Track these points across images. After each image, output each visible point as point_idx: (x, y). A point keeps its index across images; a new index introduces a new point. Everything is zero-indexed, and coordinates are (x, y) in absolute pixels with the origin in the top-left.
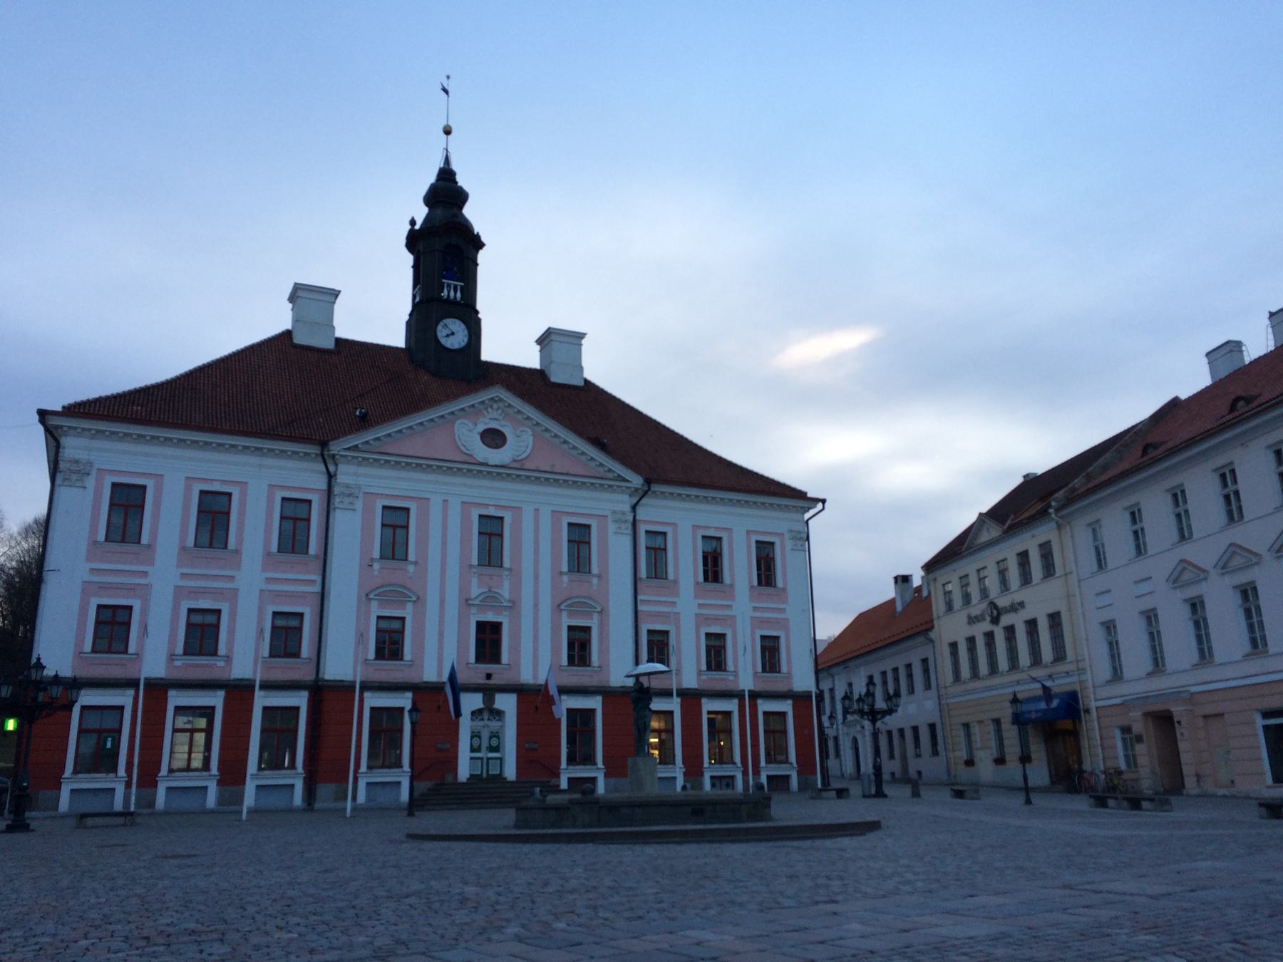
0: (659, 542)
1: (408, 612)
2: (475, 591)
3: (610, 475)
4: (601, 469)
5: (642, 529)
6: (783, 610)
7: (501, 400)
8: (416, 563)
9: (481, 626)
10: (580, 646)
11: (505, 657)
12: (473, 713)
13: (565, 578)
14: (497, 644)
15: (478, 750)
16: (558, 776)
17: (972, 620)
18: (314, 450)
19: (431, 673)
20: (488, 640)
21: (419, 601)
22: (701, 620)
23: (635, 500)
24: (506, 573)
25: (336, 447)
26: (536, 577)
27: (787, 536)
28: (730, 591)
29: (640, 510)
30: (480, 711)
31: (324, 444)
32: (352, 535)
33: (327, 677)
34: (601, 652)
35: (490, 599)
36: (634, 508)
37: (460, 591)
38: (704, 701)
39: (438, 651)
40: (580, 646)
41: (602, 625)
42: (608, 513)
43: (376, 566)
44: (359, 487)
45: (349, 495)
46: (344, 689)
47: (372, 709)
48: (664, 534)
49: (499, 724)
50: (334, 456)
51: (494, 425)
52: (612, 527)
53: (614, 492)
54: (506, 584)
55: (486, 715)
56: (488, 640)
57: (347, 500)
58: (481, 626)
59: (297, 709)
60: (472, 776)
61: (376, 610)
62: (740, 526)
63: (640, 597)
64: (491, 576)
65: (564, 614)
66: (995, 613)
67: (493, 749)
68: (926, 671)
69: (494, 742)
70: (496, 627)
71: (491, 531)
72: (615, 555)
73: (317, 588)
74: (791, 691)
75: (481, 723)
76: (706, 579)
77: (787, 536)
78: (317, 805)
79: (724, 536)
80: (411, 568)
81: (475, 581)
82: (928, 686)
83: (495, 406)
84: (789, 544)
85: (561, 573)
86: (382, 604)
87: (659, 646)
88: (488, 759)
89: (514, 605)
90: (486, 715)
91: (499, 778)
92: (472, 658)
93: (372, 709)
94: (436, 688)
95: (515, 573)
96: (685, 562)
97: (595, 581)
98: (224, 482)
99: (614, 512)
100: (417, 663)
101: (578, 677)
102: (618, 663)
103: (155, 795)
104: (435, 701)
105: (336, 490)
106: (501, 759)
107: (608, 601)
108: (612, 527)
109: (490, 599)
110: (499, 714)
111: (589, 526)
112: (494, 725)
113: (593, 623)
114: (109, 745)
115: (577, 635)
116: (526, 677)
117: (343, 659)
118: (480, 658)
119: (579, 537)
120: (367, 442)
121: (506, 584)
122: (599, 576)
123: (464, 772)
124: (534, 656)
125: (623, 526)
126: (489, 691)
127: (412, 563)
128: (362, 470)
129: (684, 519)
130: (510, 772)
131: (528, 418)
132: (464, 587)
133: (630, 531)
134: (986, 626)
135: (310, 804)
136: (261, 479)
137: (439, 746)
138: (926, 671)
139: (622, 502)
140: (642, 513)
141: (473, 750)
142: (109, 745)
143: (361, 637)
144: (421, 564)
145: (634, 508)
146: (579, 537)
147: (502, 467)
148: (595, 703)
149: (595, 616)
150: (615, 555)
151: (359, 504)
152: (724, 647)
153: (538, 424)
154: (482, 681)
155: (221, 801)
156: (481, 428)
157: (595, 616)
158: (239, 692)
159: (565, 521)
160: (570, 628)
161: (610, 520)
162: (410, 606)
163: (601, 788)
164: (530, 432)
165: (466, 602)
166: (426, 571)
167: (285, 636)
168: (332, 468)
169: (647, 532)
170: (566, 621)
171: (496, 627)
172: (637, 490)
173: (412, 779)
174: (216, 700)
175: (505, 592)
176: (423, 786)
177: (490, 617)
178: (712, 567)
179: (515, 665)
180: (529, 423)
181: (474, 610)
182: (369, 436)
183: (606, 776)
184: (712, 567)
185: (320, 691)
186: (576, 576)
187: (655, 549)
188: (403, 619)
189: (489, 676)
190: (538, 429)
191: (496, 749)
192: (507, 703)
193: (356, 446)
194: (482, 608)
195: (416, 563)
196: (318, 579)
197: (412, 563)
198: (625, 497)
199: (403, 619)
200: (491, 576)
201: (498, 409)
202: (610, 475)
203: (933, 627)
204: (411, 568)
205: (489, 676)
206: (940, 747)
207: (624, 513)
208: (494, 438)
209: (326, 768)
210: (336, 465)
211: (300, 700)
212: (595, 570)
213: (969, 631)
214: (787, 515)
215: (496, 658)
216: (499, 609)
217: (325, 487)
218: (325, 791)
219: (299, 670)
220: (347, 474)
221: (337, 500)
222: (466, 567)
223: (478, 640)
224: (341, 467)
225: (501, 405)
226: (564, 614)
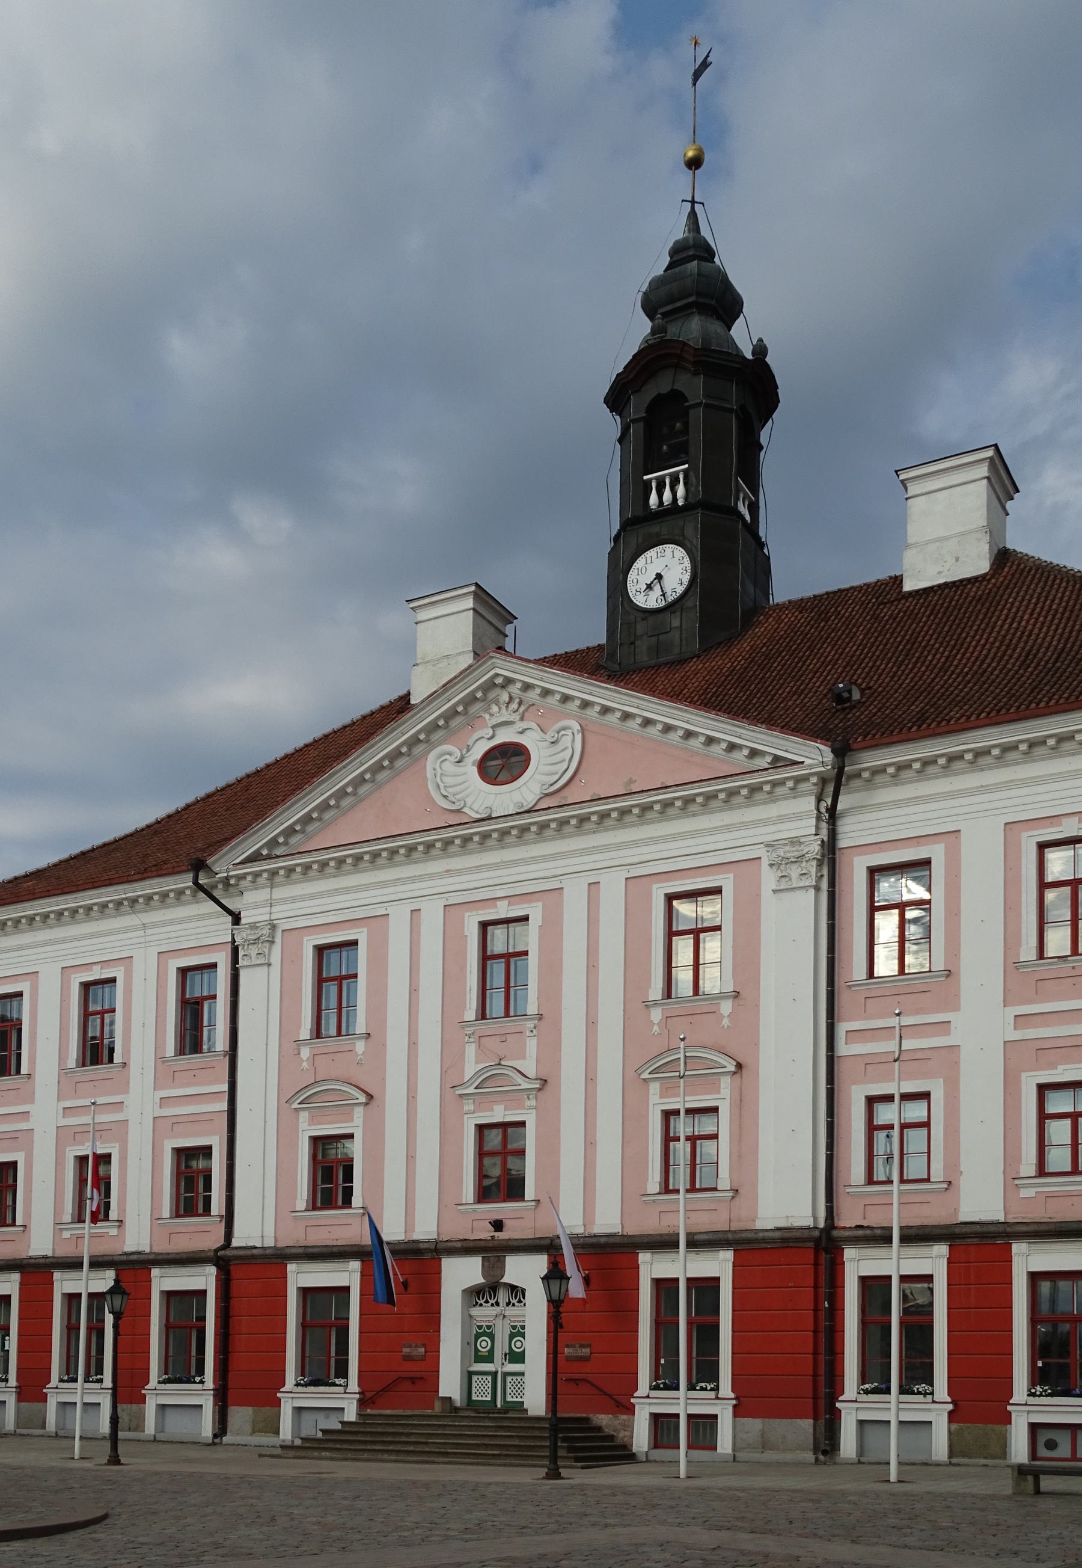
1: (356, 1123)
2: (471, 1067)
7: (509, 681)
19: (393, 1231)
26: (591, 1023)
35: (490, 1082)
37: (444, 1073)
41: (745, 1106)
42: (760, 852)
46: (274, 1261)
51: (505, 736)
59: (203, 1293)
61: (308, 1128)
64: (503, 1037)
65: (654, 1088)
81: (471, 1050)
85: (648, 1005)
95: (547, 1021)
118: (484, 1194)
131: (566, 699)
132: (450, 1062)
140: (850, 833)
143: (284, 1172)
149: (725, 1082)
162: (359, 1111)
167: (193, 1180)
177: (499, 1114)
179: (549, 1200)
181: (469, 1106)
200: (503, 1037)
208: (505, 762)
209: (246, 1384)
211: (204, 1279)
216: (514, 1096)
218: (240, 1416)
219: (204, 1234)
226: (654, 1088)
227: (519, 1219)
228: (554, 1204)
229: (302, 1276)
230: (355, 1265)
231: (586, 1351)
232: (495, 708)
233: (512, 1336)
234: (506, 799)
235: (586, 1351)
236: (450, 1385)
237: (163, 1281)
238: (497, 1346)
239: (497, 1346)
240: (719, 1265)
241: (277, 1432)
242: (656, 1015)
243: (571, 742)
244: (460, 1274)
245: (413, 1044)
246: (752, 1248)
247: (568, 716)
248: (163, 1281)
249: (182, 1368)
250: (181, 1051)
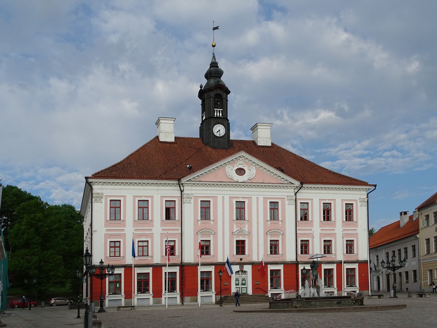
0: (305, 206)
1: (211, 238)
2: (235, 230)
3: (286, 182)
4: (283, 180)
5: (299, 202)
6: (356, 230)
7: (243, 156)
8: (213, 221)
9: (237, 241)
10: (274, 247)
11: (247, 252)
12: (236, 272)
13: (269, 223)
15: (238, 285)
16: (267, 293)
18: (176, 182)
19: (220, 259)
20: (241, 247)
21: (215, 234)
22: (322, 235)
23: (296, 192)
24: (247, 222)
25: (183, 181)
27: (358, 201)
28: (334, 225)
29: (297, 194)
30: (238, 271)
31: (179, 180)
32: (190, 212)
34: (283, 249)
35: (241, 232)
36: (296, 194)
38: (322, 265)
39: (223, 251)
40: (274, 247)
43: (199, 222)
44: (192, 194)
45: (189, 198)
47: (201, 272)
48: (308, 203)
49: (246, 276)
50: (182, 184)
52: (287, 202)
53: (288, 188)
54: (247, 226)
55: (240, 273)
56: (241, 247)
57: (188, 200)
58: (237, 241)
59: (176, 272)
60: (237, 295)
62: (338, 197)
63: (297, 228)
65: (269, 236)
67: (243, 284)
68: (414, 250)
69: (244, 282)
70: (243, 242)
71: (240, 207)
72: (289, 213)
73: (180, 232)
74: (357, 260)
75: (239, 276)
76: (324, 220)
77: (358, 201)
78: (185, 304)
79: (332, 203)
80: (212, 222)
81: (235, 226)
82: (414, 256)
83: (241, 159)
84: (359, 204)
86: (202, 236)
87: (305, 247)
88: (242, 288)
89: (250, 233)
90: (240, 273)
91: (246, 294)
92: (235, 253)
93: (201, 272)
94: (223, 264)
95: (250, 222)
96: (316, 213)
97: (280, 223)
99: (288, 196)
100: (216, 255)
101: (274, 258)
102: (289, 253)
104: (222, 268)
105: (184, 196)
107: (285, 230)
108: (287, 202)
109: (241, 232)
110: (245, 272)
111: (278, 202)
112: (244, 276)
113: (280, 239)
115: (273, 243)
116: (255, 259)
117: (190, 255)
119: (274, 207)
120: (194, 178)
121: (247, 226)
122: (282, 221)
124: (257, 252)
125: (291, 201)
126: (241, 264)
127: (212, 220)
128: (192, 188)
129: (316, 196)
130: (250, 292)
131: (254, 162)
132: (231, 228)
133: (294, 203)
135: (182, 303)
136: (159, 193)
137: (224, 284)
138: (414, 250)
139: (291, 192)
141: (236, 285)
144: (215, 221)
145: (296, 194)
146: (274, 207)
147: (244, 182)
148: (281, 267)
150: (289, 213)
151: (192, 201)
152: (331, 245)
153: (258, 164)
154: (239, 261)
156: (236, 168)
157: (280, 236)
159: (269, 201)
160: (270, 240)
161: (286, 199)
162: (212, 236)
164: (254, 168)
165: (232, 233)
166: (217, 223)
168: (182, 188)
169: (301, 203)
170: (269, 238)
171: (243, 242)
172: (297, 187)
173: (216, 295)
175: (246, 229)
177: (241, 238)
178: (327, 214)
179: (251, 255)
180: (254, 164)
181: (235, 236)
182: (195, 175)
184: (327, 214)
185: (183, 266)
186: (273, 221)
187: (304, 209)
188: (210, 241)
189: (241, 259)
190: (258, 166)
191: (244, 284)
192: (248, 268)
193: (190, 179)
194: (238, 235)
195: (213, 221)
196: (180, 228)
197: (212, 220)
198: (293, 190)
199: (210, 241)
201: (242, 159)
202: (286, 182)
203: (419, 233)
204: (212, 222)
205: (241, 259)
206: (418, 278)
207: (291, 196)
208: (241, 172)
210: (183, 187)
212: (280, 219)
214: (359, 192)
215: (243, 253)
216: (244, 235)
217: (180, 195)
219: (175, 259)
220: (187, 190)
221: (185, 200)
222: (231, 221)
223: (237, 247)
224: (185, 187)
225: (243, 158)
226: (269, 236)
227: (245, 258)
228: (252, 255)
229: (201, 269)
230: (213, 267)
231: (259, 283)
232: (239, 161)
233: (242, 280)
234: (241, 179)
235: (259, 283)
236: (234, 290)
237: (166, 270)
238: (242, 282)
239: (242, 282)
240: (281, 267)
241: (197, 301)
242: (269, 223)
243: (254, 171)
244: (236, 268)
245: (223, 223)
246: (286, 265)
247: (252, 166)
248: (166, 270)
249: (172, 289)
250: (166, 219)
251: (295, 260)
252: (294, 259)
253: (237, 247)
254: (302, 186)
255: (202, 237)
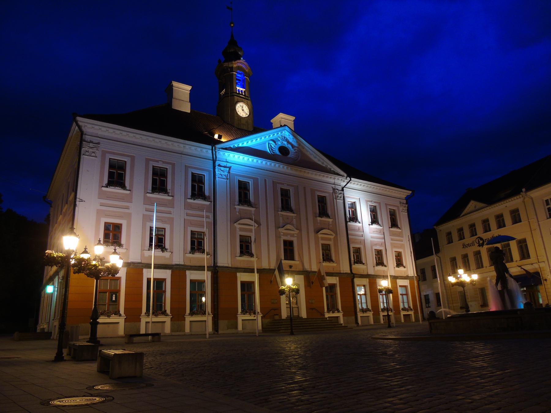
9: (285, 242)
14: (292, 251)
16: (324, 315)
17: (464, 246)
19: (265, 265)
33: (219, 265)
47: (241, 282)
58: (285, 242)
66: (481, 242)
91: (299, 317)
98: (164, 162)
103: (139, 326)
106: (298, 308)
113: (331, 243)
114: (114, 299)
123: (284, 314)
134: (476, 248)
142: (114, 299)
155: (172, 330)
158: (178, 271)
163: (342, 321)
167: (197, 244)
173: (262, 317)
174: (166, 274)
176: (267, 321)
177: (288, 238)
183: (344, 315)
213: (464, 252)
241: (236, 327)
251: (348, 271)
252: (348, 271)
253: (285, 250)
254: (351, 180)
255: (241, 229)
